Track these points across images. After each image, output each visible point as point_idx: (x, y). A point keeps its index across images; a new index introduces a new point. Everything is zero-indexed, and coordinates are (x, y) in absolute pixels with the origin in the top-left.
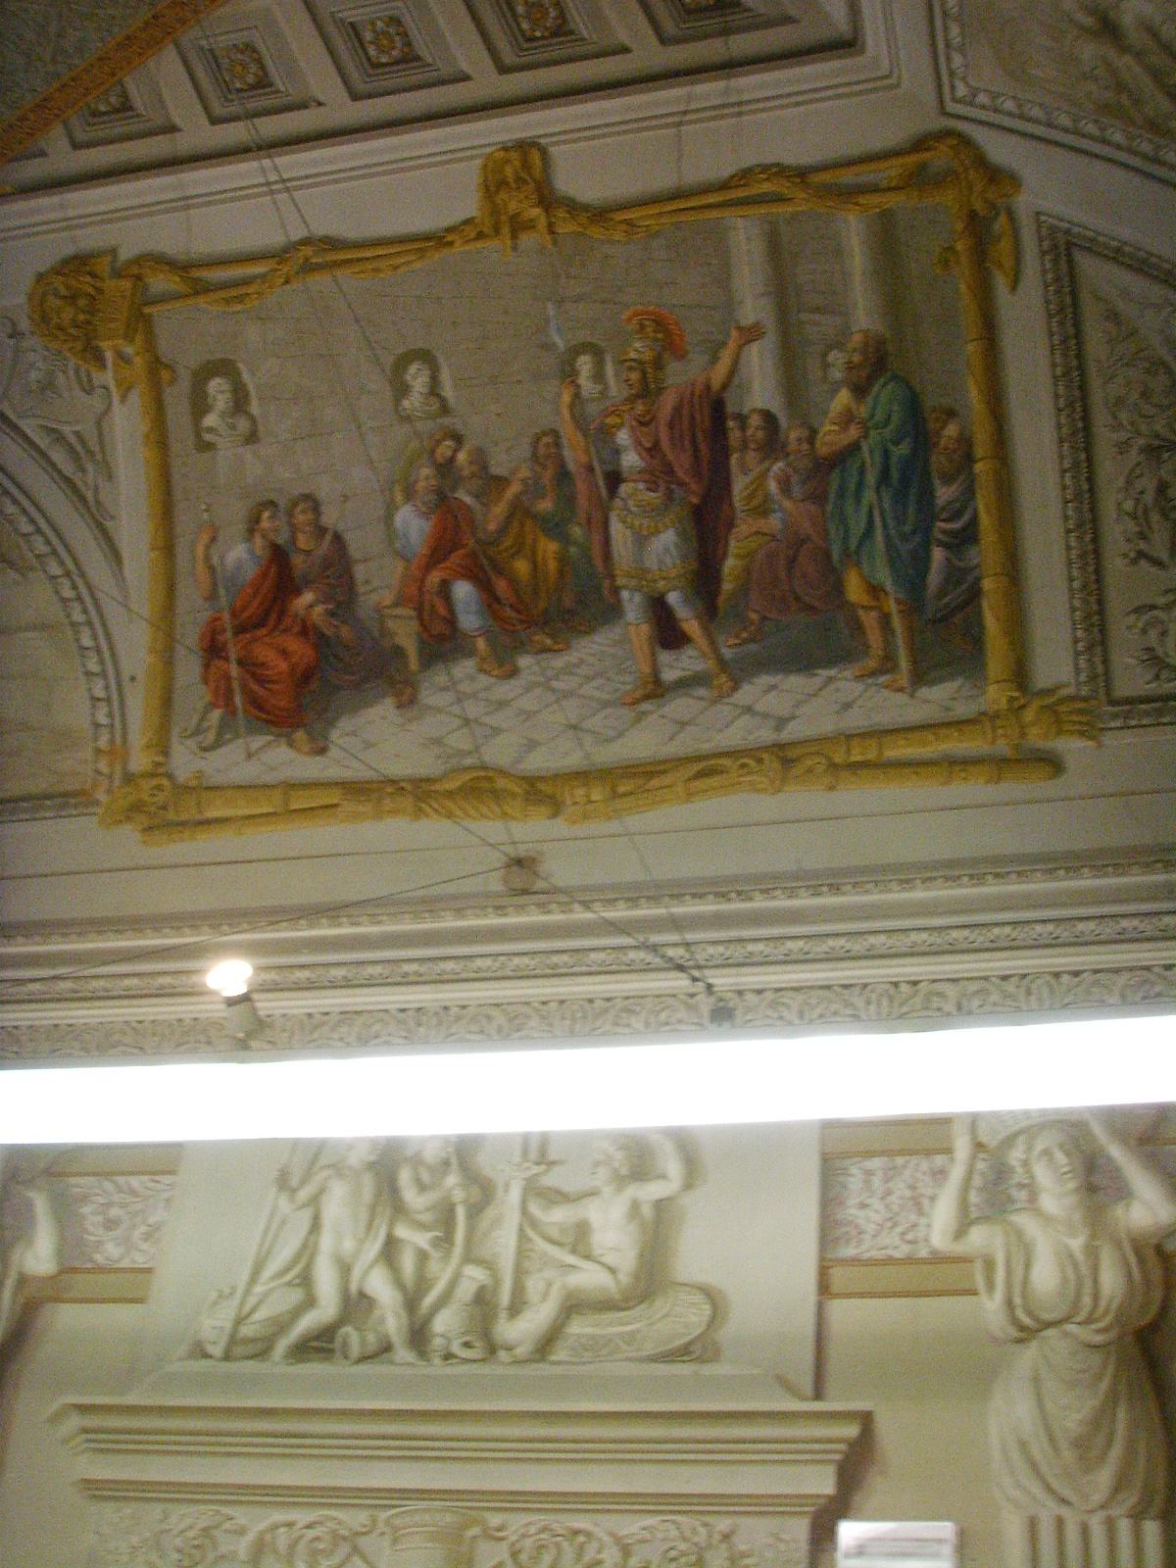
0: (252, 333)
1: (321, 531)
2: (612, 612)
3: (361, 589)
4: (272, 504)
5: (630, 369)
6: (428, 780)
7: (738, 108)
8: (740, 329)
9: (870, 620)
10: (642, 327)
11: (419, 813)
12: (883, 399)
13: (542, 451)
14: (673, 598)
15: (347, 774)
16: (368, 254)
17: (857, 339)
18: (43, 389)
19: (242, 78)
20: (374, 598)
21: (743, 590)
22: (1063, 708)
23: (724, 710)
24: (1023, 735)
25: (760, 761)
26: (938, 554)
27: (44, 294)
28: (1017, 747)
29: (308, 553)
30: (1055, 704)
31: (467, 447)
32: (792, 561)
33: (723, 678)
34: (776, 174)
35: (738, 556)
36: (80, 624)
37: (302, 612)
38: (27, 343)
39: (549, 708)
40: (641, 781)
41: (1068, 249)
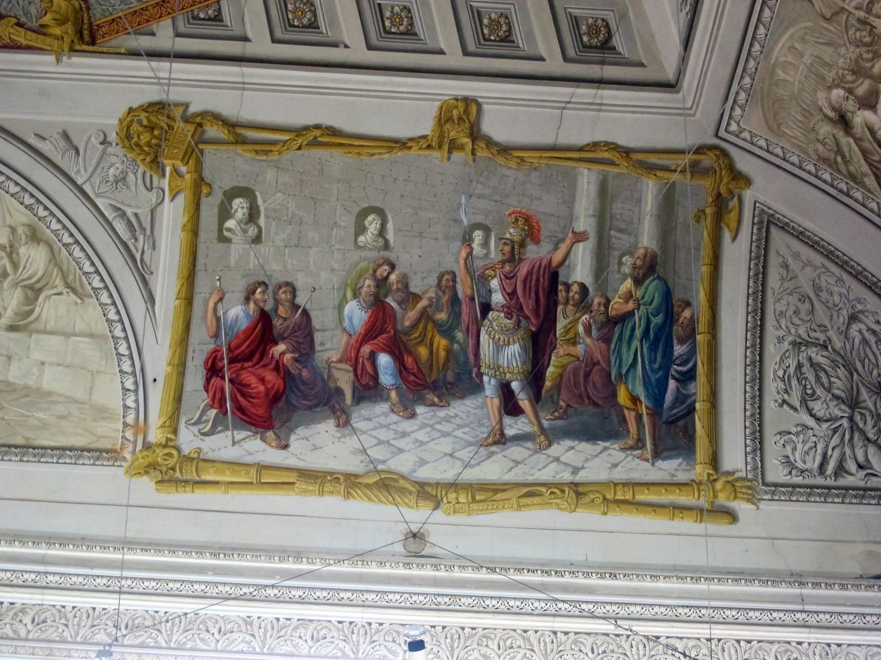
0: (270, 175)
1: (296, 307)
2: (478, 388)
3: (318, 348)
4: (264, 283)
5: (505, 244)
6: (356, 476)
7: (601, 107)
8: (573, 232)
9: (630, 416)
10: (517, 220)
11: (348, 495)
12: (651, 289)
13: (444, 282)
14: (515, 385)
15: (301, 464)
16: (356, 143)
17: (641, 252)
18: (117, 183)
19: (300, 20)
20: (326, 355)
21: (558, 387)
22: (738, 484)
23: (541, 458)
24: (715, 496)
25: (563, 491)
26: (672, 384)
27: (132, 121)
28: (712, 503)
29: (285, 319)
30: (733, 481)
31: (397, 272)
32: (587, 375)
33: (542, 438)
34: (613, 149)
35: (556, 367)
36: (120, 338)
37: (277, 356)
38: (110, 150)
39: (436, 440)
40: (490, 494)
41: (768, 225)
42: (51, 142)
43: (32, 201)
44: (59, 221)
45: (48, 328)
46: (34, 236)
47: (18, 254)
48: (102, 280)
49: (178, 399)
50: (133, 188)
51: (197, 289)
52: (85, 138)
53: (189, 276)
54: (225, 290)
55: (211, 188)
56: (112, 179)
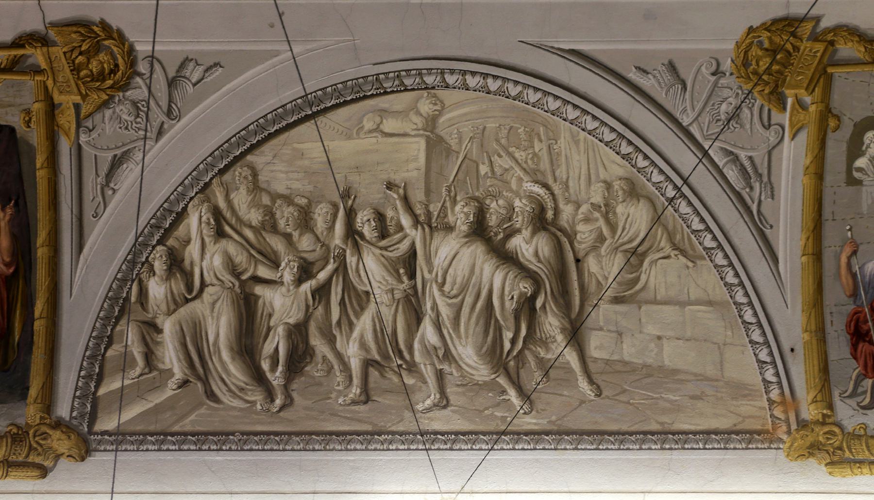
36: (743, 304)
38: (723, 81)
42: (654, 77)
43: (630, 149)
44: (661, 172)
45: (659, 298)
46: (633, 192)
47: (615, 213)
48: (715, 238)
49: (825, 370)
50: (748, 126)
51: (826, 243)
52: (694, 69)
53: (815, 228)
54: (859, 242)
55: (839, 120)
56: (723, 117)
